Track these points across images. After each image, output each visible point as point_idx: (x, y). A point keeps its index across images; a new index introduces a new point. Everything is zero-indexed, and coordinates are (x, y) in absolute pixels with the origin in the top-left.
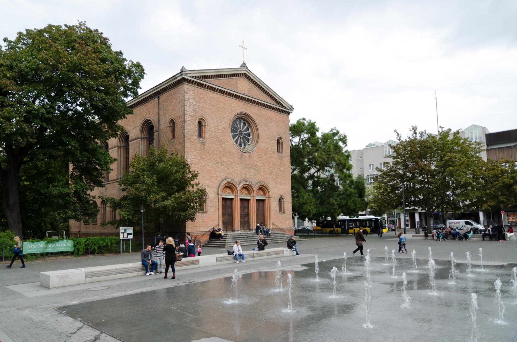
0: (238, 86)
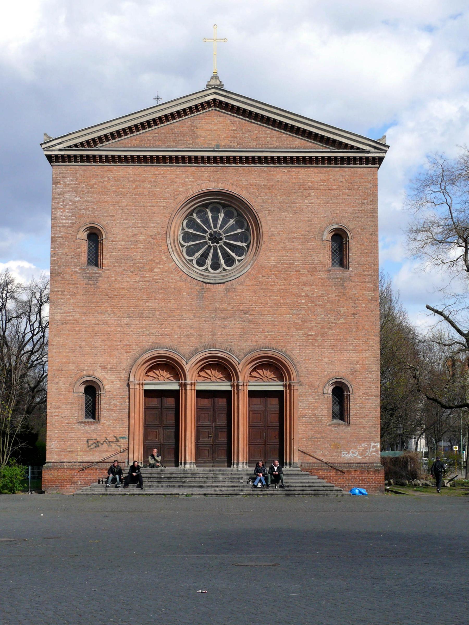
0: (199, 132)
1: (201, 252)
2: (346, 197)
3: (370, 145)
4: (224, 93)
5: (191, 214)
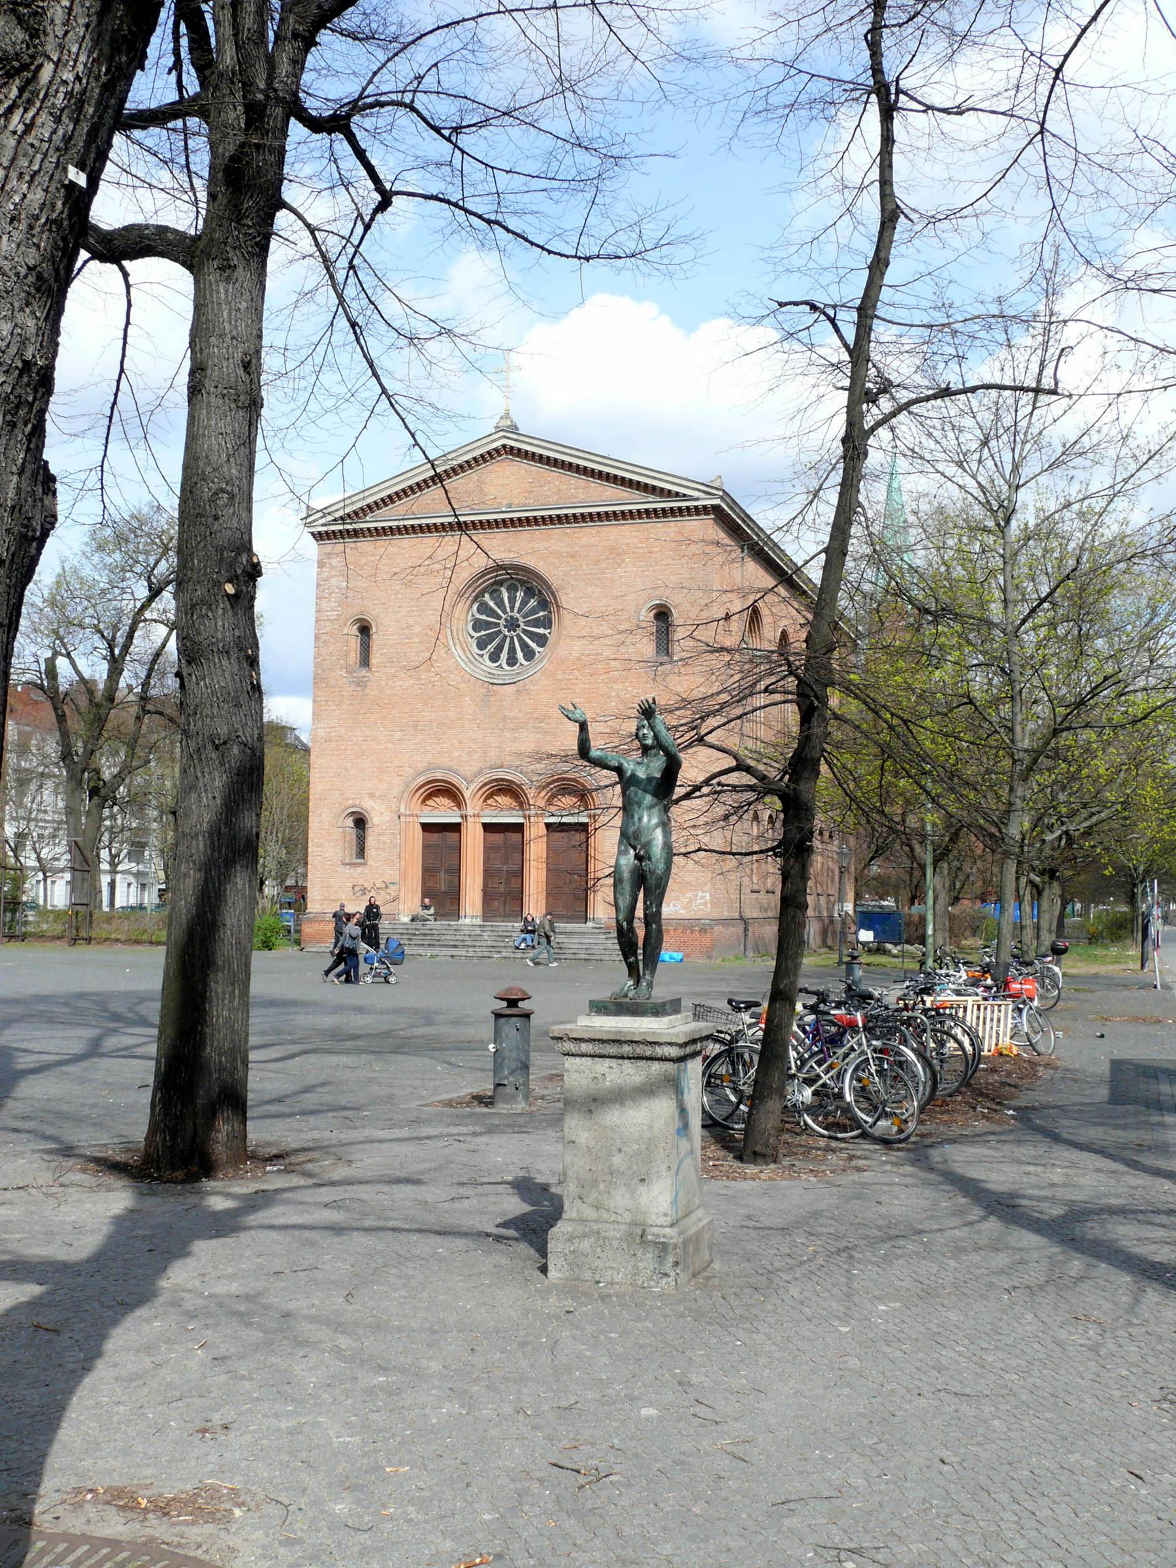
1: (494, 644)
2: (670, 561)
3: (699, 490)
4: (515, 436)
5: (481, 594)
